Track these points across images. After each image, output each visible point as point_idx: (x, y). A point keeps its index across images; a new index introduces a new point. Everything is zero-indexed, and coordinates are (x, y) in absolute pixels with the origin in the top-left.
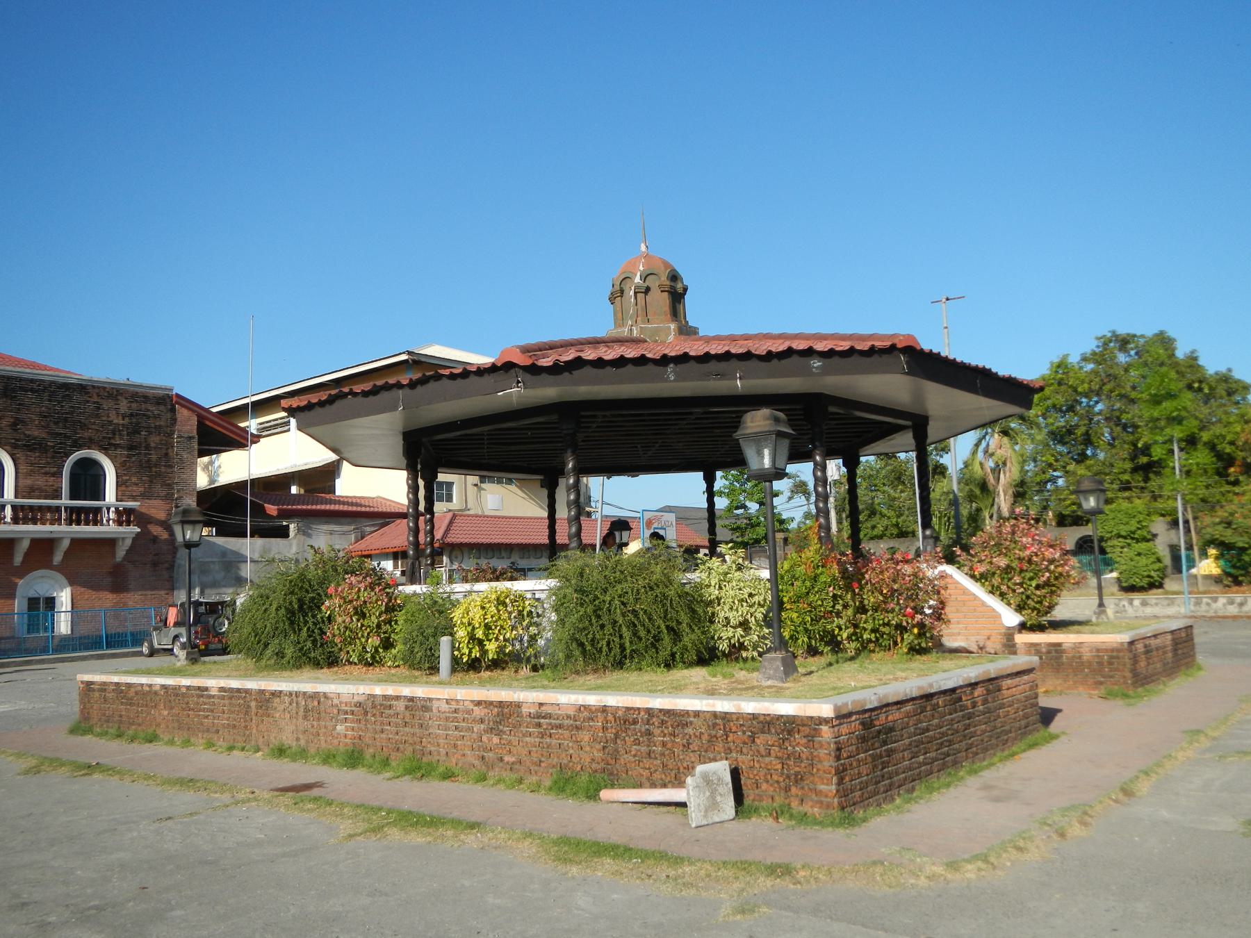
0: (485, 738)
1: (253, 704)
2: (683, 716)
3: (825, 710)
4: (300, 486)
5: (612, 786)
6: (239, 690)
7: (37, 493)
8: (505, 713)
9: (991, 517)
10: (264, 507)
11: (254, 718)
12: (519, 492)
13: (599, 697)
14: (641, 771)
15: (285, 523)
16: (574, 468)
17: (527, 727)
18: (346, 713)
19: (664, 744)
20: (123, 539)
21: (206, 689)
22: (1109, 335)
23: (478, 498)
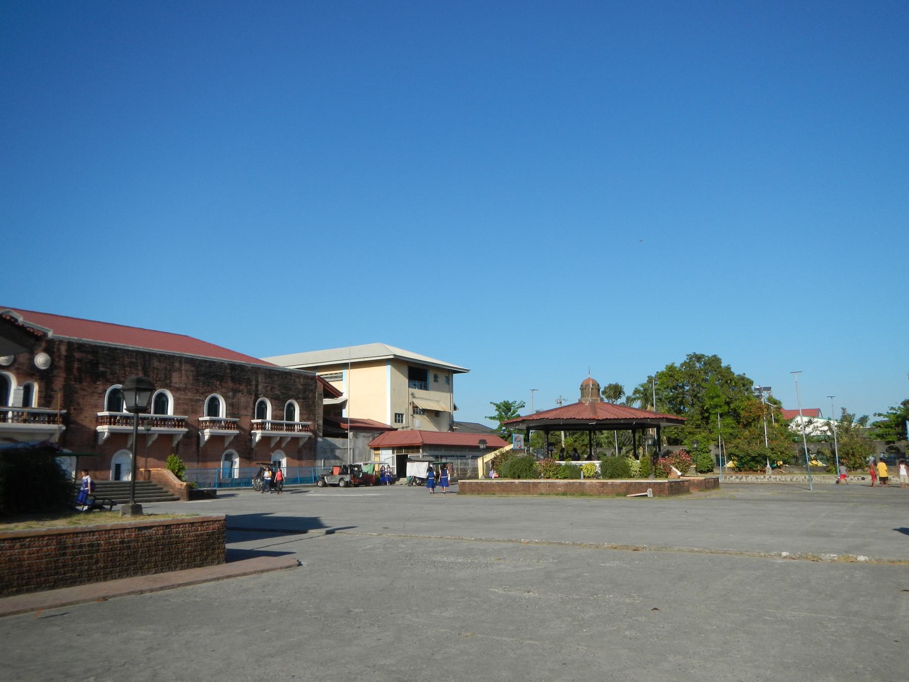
1: (531, 485)
3: (667, 481)
7: (277, 418)
10: (340, 425)
12: (427, 419)
20: (305, 438)
22: (693, 354)
23: (413, 421)
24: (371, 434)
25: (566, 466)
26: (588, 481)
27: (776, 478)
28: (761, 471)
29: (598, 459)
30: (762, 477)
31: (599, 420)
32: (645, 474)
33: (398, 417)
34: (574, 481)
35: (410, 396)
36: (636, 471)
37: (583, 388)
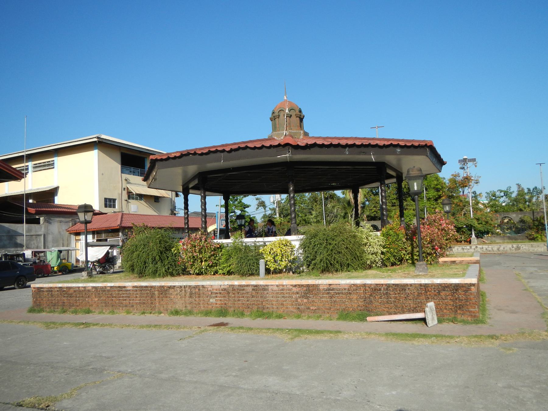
0: (299, 300)
1: (156, 293)
2: (405, 286)
4: (34, 199)
5: (370, 316)
6: (146, 287)
8: (310, 290)
9: (351, 216)
11: (157, 299)
13: (362, 281)
14: (384, 309)
15: (37, 217)
16: (293, 189)
17: (323, 294)
18: (217, 293)
19: (396, 298)
21: (125, 287)
23: (127, 206)
24: (71, 219)
25: (237, 249)
26: (273, 282)
27: (482, 248)
28: (465, 241)
29: (298, 233)
30: (468, 247)
31: (297, 147)
32: (392, 259)
33: (109, 202)
34: (244, 282)
35: (124, 181)
36: (376, 254)
37: (274, 118)
